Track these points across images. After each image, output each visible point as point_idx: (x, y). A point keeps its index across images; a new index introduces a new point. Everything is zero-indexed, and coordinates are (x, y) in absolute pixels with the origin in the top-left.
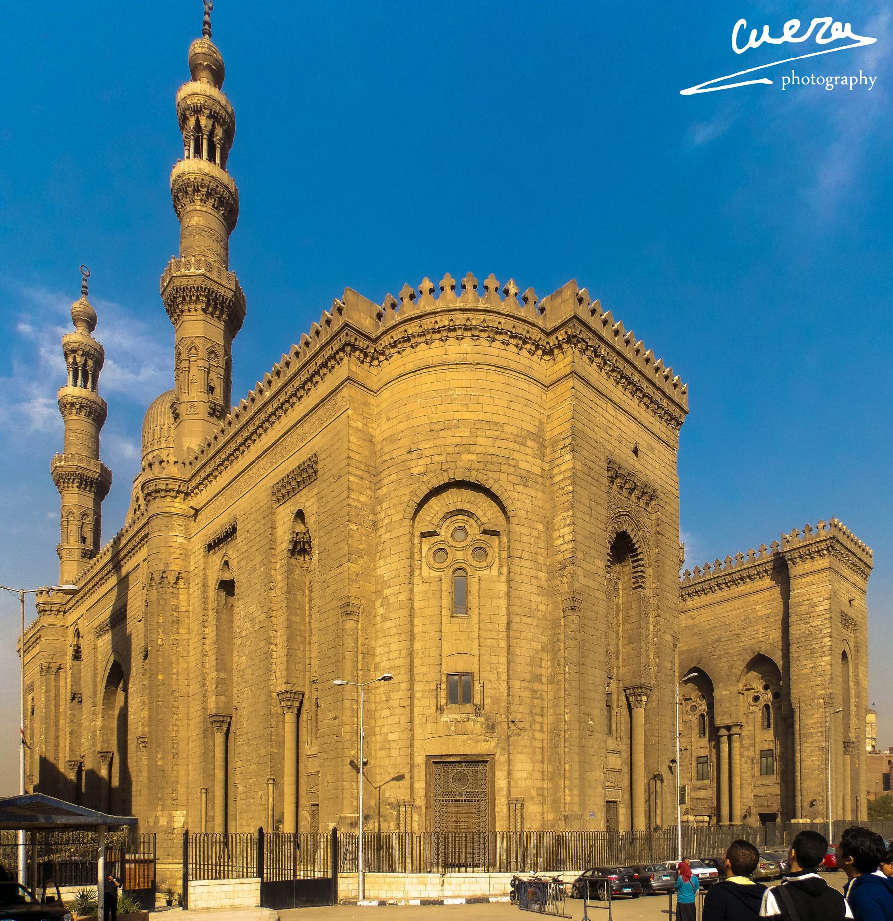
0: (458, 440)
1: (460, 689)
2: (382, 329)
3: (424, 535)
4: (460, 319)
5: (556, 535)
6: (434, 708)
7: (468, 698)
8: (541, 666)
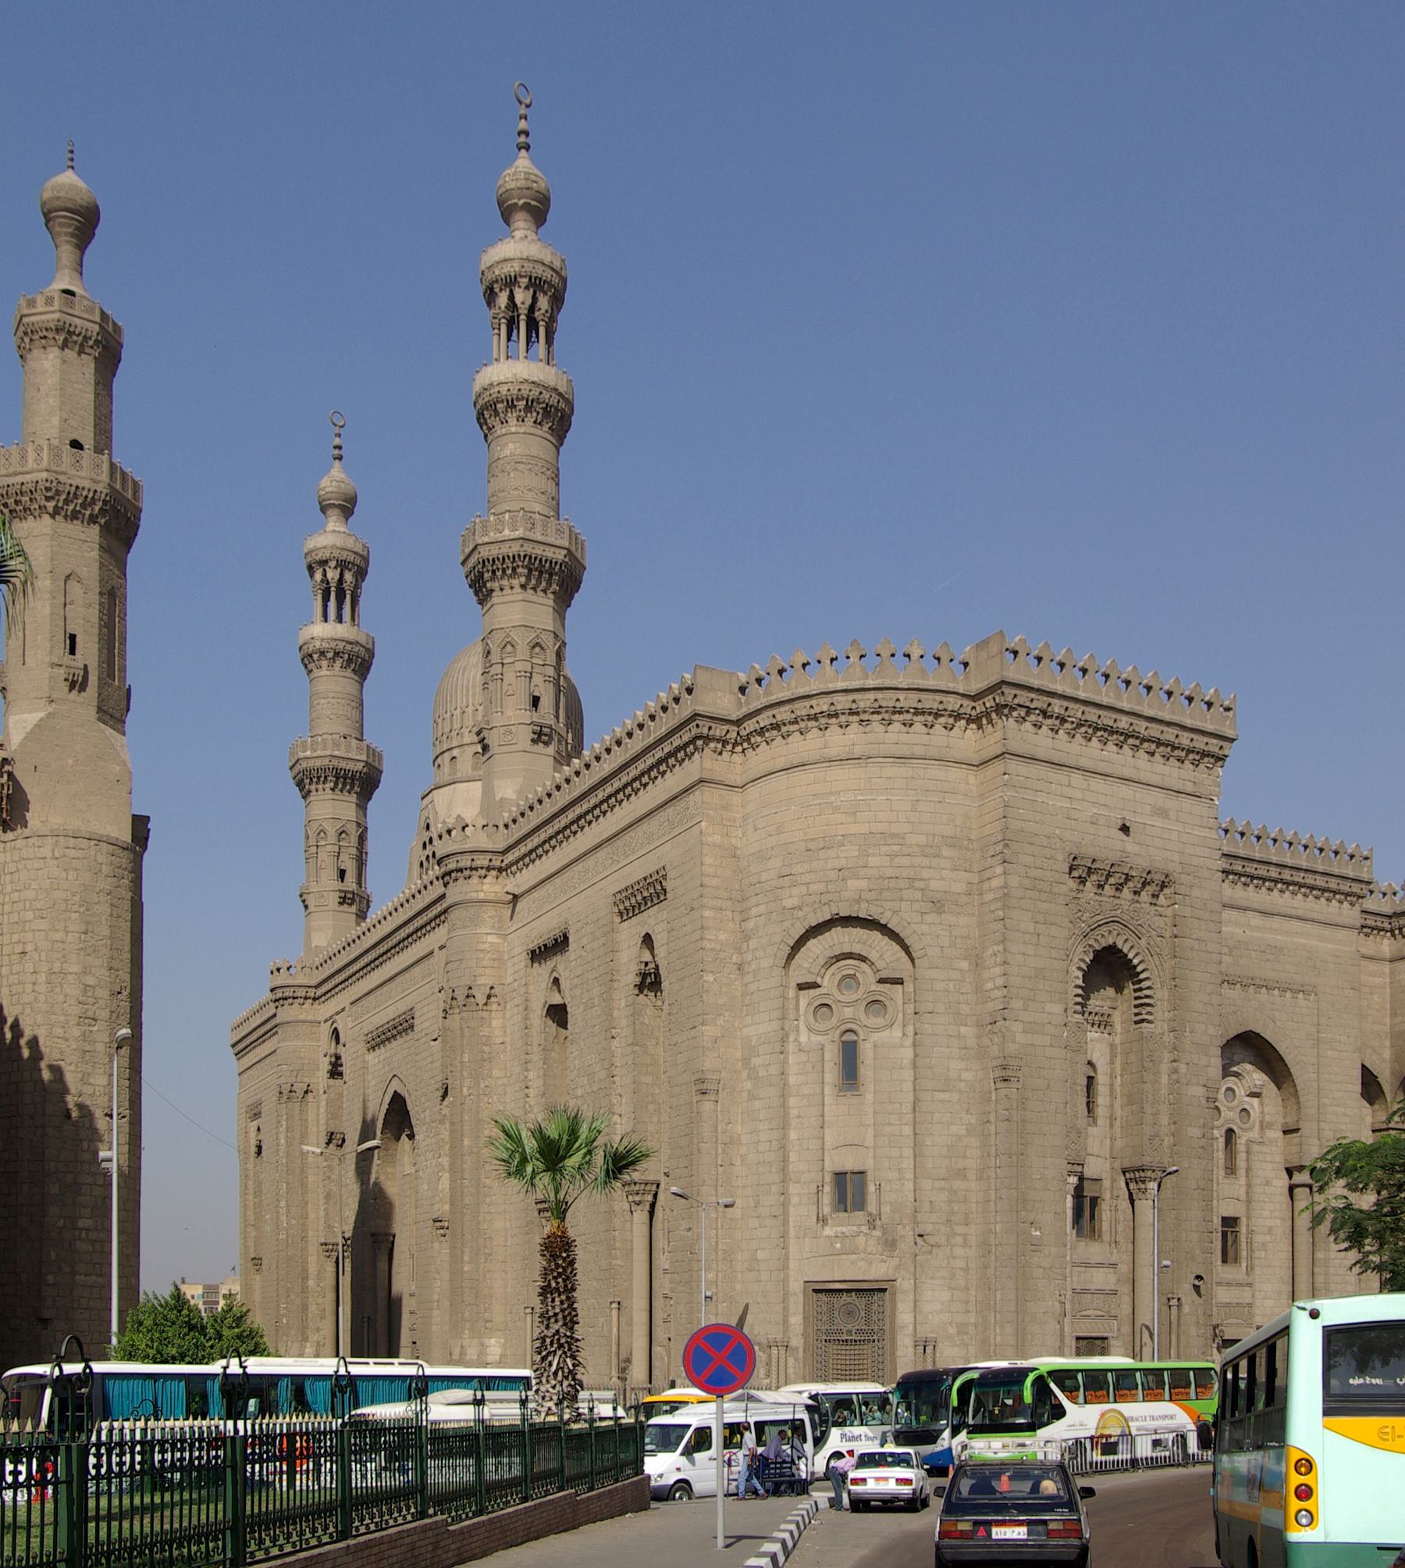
0: (843, 863)
1: (848, 1190)
2: (744, 711)
3: (802, 987)
4: (842, 702)
5: (986, 975)
6: (815, 1219)
7: (860, 1204)
8: (965, 1157)
